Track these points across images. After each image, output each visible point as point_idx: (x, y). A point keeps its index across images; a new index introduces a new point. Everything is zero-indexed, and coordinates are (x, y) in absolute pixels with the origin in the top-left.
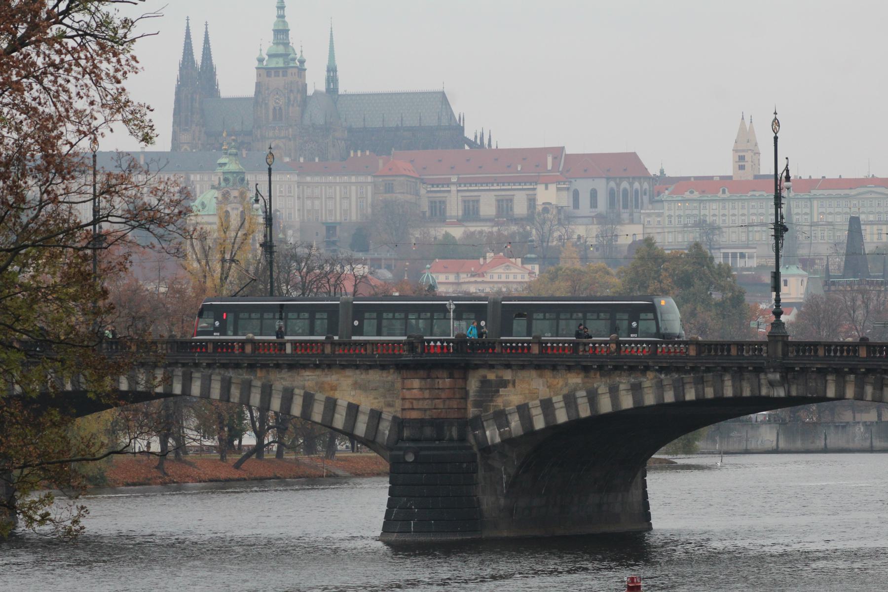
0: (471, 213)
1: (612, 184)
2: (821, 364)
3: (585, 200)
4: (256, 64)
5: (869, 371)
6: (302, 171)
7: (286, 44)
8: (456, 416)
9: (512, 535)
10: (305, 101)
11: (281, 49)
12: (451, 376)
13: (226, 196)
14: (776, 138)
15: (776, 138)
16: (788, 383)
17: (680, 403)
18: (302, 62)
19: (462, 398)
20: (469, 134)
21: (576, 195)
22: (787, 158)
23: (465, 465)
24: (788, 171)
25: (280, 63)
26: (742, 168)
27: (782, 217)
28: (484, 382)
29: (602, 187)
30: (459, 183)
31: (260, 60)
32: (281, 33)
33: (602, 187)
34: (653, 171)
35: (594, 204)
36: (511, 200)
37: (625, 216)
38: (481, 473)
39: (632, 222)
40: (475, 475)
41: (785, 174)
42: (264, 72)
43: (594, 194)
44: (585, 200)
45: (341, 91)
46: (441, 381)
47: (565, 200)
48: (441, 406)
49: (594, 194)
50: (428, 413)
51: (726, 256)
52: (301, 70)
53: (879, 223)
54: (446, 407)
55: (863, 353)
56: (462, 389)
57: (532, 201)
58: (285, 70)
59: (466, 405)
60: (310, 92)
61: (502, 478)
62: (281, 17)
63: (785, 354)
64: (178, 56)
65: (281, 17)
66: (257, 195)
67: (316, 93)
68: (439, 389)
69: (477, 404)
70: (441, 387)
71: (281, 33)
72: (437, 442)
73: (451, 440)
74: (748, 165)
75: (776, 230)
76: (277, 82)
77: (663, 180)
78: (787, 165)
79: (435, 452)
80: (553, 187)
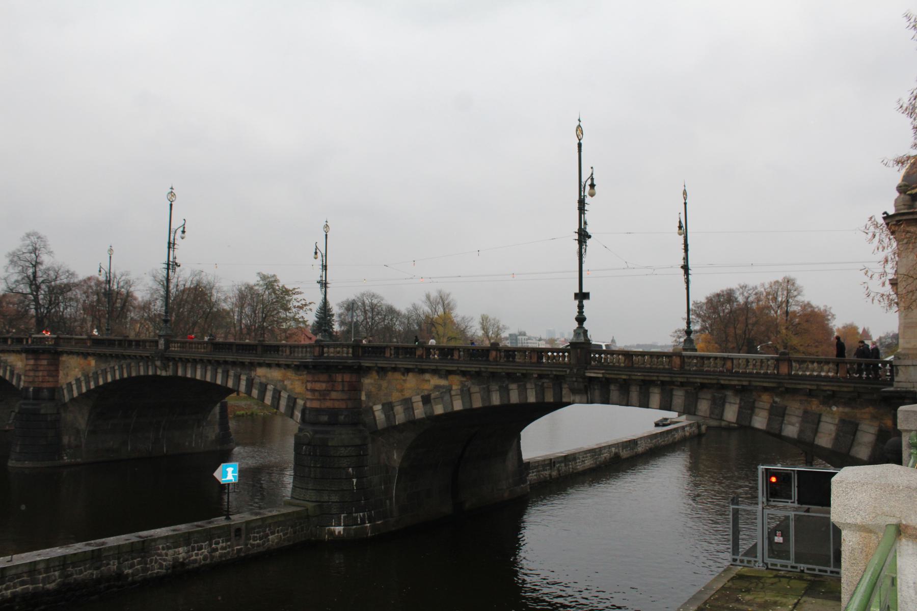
14: (171, 205)
22: (184, 220)
24: (184, 228)
27: (175, 258)
41: (182, 229)
75: (168, 264)
78: (184, 224)
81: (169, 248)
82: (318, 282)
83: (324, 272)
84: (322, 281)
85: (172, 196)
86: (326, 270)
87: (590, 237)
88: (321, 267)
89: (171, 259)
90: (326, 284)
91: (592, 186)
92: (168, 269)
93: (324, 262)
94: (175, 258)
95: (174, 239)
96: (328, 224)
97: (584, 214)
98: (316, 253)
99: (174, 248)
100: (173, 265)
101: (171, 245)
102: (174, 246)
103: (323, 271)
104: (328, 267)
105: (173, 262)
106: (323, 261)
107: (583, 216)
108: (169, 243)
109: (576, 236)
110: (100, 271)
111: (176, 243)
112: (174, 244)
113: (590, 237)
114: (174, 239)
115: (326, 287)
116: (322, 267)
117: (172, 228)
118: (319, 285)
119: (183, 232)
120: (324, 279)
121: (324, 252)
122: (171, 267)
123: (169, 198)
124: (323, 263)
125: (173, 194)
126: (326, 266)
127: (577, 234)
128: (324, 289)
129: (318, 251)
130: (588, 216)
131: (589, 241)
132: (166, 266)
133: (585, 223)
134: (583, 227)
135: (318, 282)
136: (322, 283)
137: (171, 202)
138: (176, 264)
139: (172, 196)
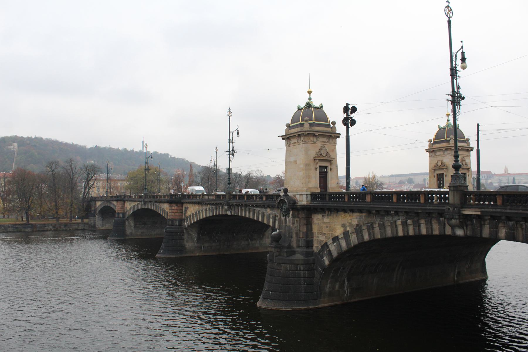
1: (487, 175)
2: (235, 202)
3: (483, 177)
5: (246, 206)
8: (178, 218)
9: (201, 255)
12: (177, 206)
14: (229, 118)
15: (229, 118)
16: (231, 210)
17: (213, 216)
19: (181, 212)
22: (238, 126)
23: (179, 233)
24: (238, 131)
26: (506, 172)
28: (185, 207)
29: (486, 175)
33: (486, 175)
34: (493, 173)
35: (485, 177)
37: (489, 179)
38: (186, 236)
39: (490, 180)
40: (183, 237)
41: (237, 131)
43: (485, 176)
44: (483, 177)
46: (174, 207)
48: (173, 215)
49: (485, 176)
50: (171, 217)
51: (503, 184)
53: (525, 179)
54: (175, 215)
55: (368, 199)
56: (181, 209)
59: (183, 214)
61: (194, 238)
63: (230, 199)
68: (173, 210)
69: (184, 215)
70: (174, 209)
72: (172, 226)
73: (176, 225)
74: (506, 172)
75: (229, 152)
77: (495, 174)
79: (173, 229)
81: (229, 142)
85: (230, 113)
87: (463, 98)
89: (231, 148)
91: (463, 60)
92: (229, 154)
94: (233, 148)
95: (232, 137)
97: (456, 79)
99: (232, 142)
100: (232, 152)
101: (230, 141)
102: (232, 141)
105: (232, 151)
107: (455, 81)
108: (229, 140)
109: (450, 98)
111: (233, 139)
112: (232, 140)
113: (463, 98)
114: (232, 137)
117: (230, 131)
119: (238, 133)
122: (231, 153)
123: (228, 114)
125: (230, 112)
127: (450, 96)
130: (460, 81)
131: (462, 102)
132: (228, 153)
133: (458, 88)
134: (456, 90)
137: (229, 117)
138: (234, 152)
139: (230, 113)
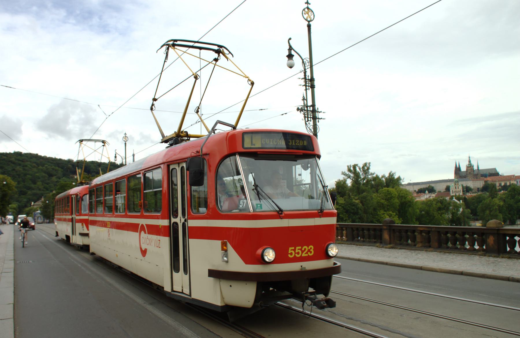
0: (500, 185)
4: (466, 166)
6: (473, 181)
7: (470, 163)
10: (474, 171)
11: (470, 164)
13: (455, 184)
18: (473, 165)
20: (500, 174)
21: (517, 182)
25: (469, 166)
30: (498, 181)
31: (467, 165)
32: (470, 161)
36: (506, 183)
42: (467, 167)
45: (480, 169)
47: (515, 183)
52: (473, 166)
57: (510, 183)
58: (470, 167)
60: (475, 169)
62: (469, 159)
64: (454, 166)
65: (469, 159)
66: (116, 154)
67: (476, 170)
71: (470, 161)
76: (469, 168)
80: (513, 181)
82: (298, 109)
83: (309, 92)
84: (307, 107)
86: (313, 87)
88: (302, 82)
90: (314, 111)
93: (308, 73)
96: (310, 6)
98: (290, 56)
103: (306, 90)
104: (316, 83)
106: (305, 73)
110: (116, 157)
115: (315, 118)
116: (306, 82)
118: (301, 115)
120: (310, 103)
121: (306, 55)
124: (305, 76)
126: (312, 80)
128: (312, 123)
129: (293, 53)
135: (298, 109)
136: (307, 110)
